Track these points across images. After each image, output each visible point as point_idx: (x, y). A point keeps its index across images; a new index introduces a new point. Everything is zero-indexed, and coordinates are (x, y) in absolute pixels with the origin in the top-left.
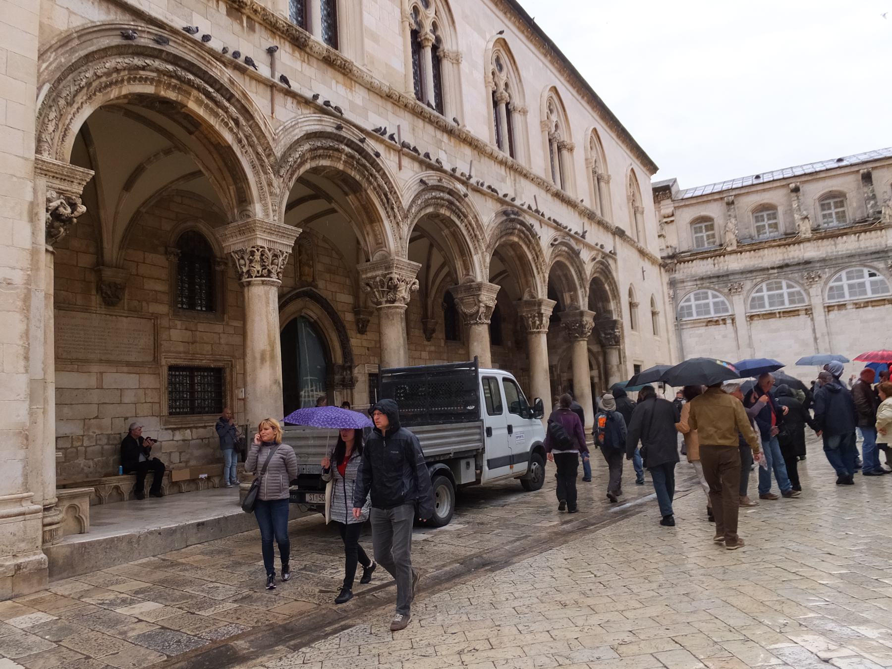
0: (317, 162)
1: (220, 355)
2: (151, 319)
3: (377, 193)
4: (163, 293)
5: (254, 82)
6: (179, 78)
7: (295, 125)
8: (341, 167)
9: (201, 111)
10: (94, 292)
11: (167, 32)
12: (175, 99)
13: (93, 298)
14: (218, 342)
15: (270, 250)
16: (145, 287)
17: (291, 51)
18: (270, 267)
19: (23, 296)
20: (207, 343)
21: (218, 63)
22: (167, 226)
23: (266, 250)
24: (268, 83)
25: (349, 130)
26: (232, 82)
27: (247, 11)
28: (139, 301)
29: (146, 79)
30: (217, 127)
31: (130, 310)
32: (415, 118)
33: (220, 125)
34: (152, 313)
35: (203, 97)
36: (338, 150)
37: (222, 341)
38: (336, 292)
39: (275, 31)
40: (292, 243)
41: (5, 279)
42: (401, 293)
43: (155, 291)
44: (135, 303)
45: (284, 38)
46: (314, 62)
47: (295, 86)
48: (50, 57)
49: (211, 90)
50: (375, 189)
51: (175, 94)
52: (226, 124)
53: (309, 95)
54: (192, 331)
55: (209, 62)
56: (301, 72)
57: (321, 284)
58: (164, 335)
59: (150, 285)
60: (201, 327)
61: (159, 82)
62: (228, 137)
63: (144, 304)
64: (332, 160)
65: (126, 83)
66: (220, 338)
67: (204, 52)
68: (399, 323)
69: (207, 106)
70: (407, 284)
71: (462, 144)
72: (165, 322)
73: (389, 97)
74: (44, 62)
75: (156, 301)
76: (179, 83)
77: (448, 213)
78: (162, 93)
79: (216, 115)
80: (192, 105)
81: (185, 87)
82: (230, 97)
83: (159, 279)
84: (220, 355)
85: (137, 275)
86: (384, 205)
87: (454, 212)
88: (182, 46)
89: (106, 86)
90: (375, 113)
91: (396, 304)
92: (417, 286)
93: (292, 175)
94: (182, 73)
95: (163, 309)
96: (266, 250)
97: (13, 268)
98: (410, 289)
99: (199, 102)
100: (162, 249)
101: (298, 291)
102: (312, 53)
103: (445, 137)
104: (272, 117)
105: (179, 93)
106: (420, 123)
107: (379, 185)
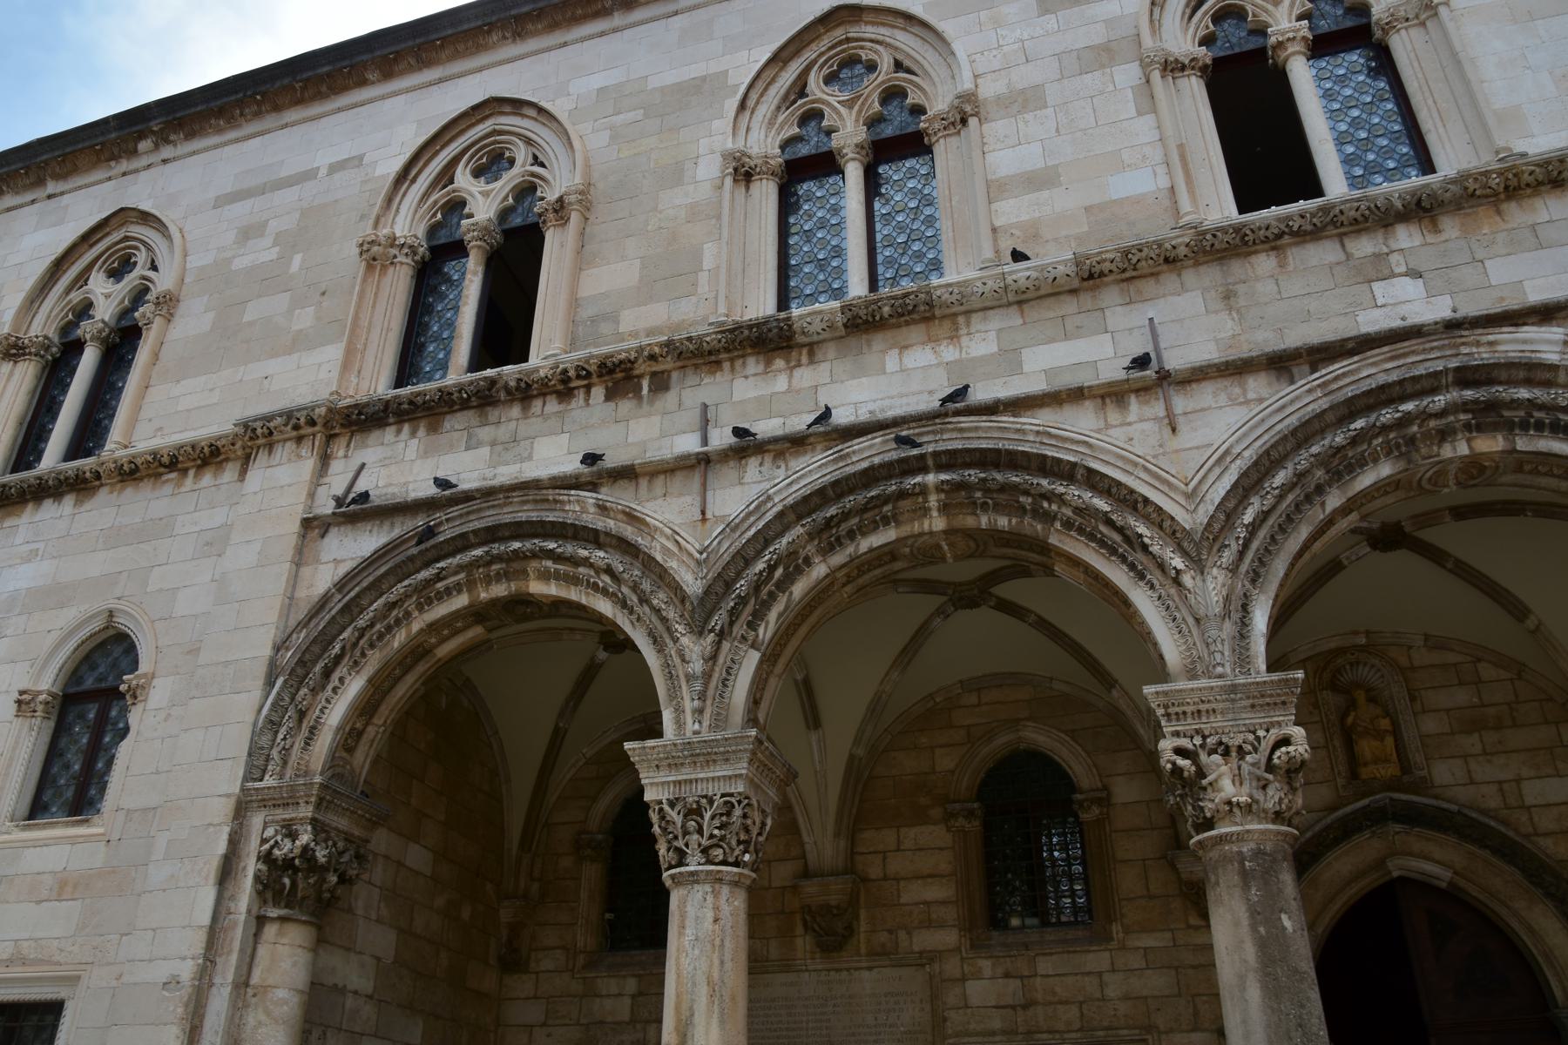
0: (850, 550)
1: (1107, 1029)
2: (923, 965)
3: (1081, 531)
4: (943, 903)
5: (660, 480)
6: (498, 558)
7: (764, 502)
8: (938, 523)
9: (552, 590)
10: (800, 930)
11: (478, 501)
12: (506, 593)
13: (799, 942)
14: (1098, 995)
15: (672, 804)
16: (902, 901)
17: (761, 368)
18: (680, 843)
19: (185, 999)
20: (1066, 1003)
21: (573, 492)
22: (946, 761)
23: (666, 807)
24: (688, 463)
25: (942, 432)
26: (603, 509)
27: (641, 368)
28: (890, 932)
29: (448, 592)
30: (584, 601)
31: (872, 954)
32: (1237, 268)
33: (587, 594)
34: (921, 953)
35: (549, 563)
36: (902, 495)
37: (1111, 992)
38: (1518, 781)
39: (713, 358)
40: (742, 767)
41: (174, 976)
42: (1220, 790)
43: (926, 903)
44: (883, 937)
45: (739, 357)
46: (831, 350)
47: (765, 428)
48: (298, 638)
49: (552, 545)
50: (1068, 525)
51: (504, 586)
52: (595, 587)
53: (800, 422)
54: (1022, 977)
55: (556, 501)
56: (789, 391)
57: (1444, 773)
58: (952, 997)
59: (914, 893)
60: (1045, 965)
61: (471, 584)
62: (605, 607)
63: (902, 935)
64: (898, 524)
65: (416, 614)
66: (1102, 985)
67: (544, 492)
68: (1237, 892)
69: (557, 576)
70: (1242, 753)
71: (1511, 208)
72: (952, 967)
73: (1091, 276)
74: (287, 649)
75: (929, 924)
76: (504, 565)
77: (1491, 444)
78: (483, 595)
79: (575, 581)
80: (536, 587)
81: (516, 565)
82: (594, 538)
83: (931, 876)
84: (1107, 1029)
85: (885, 878)
86: (1113, 551)
87: (1509, 427)
88: (505, 505)
89: (381, 636)
90: (1052, 340)
91: (1223, 829)
92: (1300, 745)
93: (758, 616)
94: (498, 548)
95: (948, 938)
96: (666, 807)
97: (184, 959)
98: (1270, 768)
99: (545, 576)
100: (936, 812)
101: (1349, 809)
102: (815, 338)
103: (1406, 237)
104: (704, 520)
105: (509, 580)
106: (1264, 263)
107: (1078, 511)
